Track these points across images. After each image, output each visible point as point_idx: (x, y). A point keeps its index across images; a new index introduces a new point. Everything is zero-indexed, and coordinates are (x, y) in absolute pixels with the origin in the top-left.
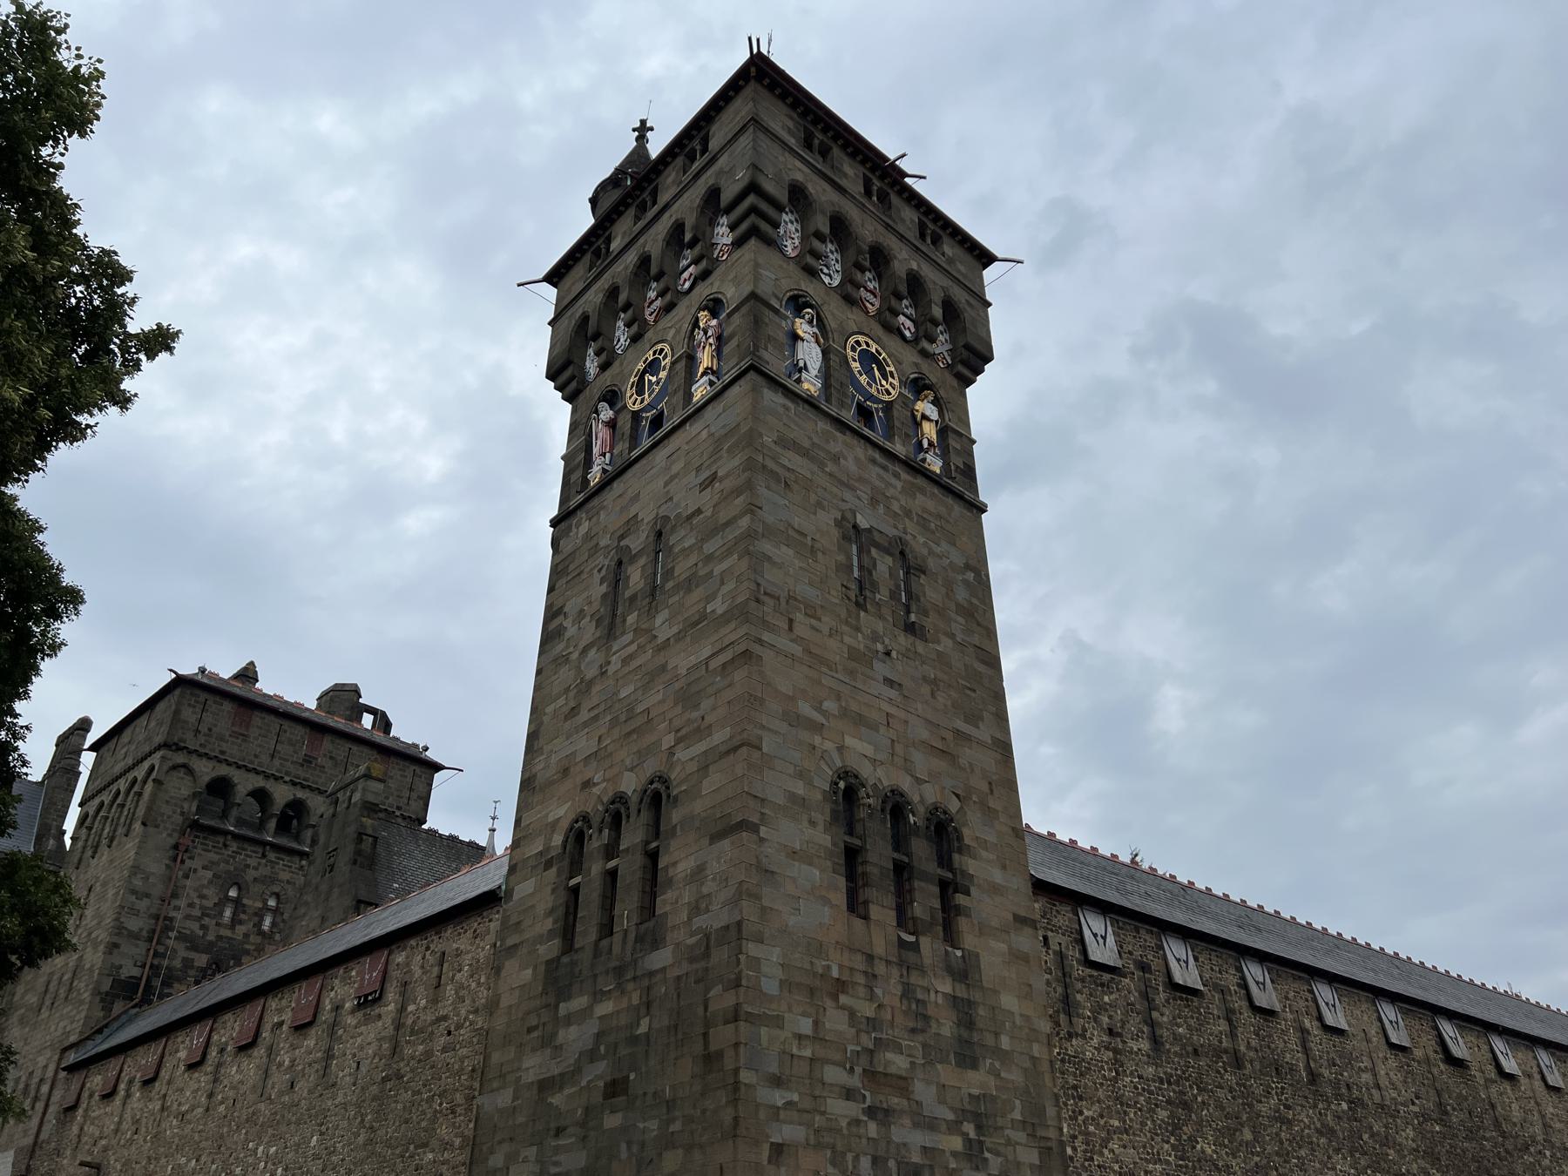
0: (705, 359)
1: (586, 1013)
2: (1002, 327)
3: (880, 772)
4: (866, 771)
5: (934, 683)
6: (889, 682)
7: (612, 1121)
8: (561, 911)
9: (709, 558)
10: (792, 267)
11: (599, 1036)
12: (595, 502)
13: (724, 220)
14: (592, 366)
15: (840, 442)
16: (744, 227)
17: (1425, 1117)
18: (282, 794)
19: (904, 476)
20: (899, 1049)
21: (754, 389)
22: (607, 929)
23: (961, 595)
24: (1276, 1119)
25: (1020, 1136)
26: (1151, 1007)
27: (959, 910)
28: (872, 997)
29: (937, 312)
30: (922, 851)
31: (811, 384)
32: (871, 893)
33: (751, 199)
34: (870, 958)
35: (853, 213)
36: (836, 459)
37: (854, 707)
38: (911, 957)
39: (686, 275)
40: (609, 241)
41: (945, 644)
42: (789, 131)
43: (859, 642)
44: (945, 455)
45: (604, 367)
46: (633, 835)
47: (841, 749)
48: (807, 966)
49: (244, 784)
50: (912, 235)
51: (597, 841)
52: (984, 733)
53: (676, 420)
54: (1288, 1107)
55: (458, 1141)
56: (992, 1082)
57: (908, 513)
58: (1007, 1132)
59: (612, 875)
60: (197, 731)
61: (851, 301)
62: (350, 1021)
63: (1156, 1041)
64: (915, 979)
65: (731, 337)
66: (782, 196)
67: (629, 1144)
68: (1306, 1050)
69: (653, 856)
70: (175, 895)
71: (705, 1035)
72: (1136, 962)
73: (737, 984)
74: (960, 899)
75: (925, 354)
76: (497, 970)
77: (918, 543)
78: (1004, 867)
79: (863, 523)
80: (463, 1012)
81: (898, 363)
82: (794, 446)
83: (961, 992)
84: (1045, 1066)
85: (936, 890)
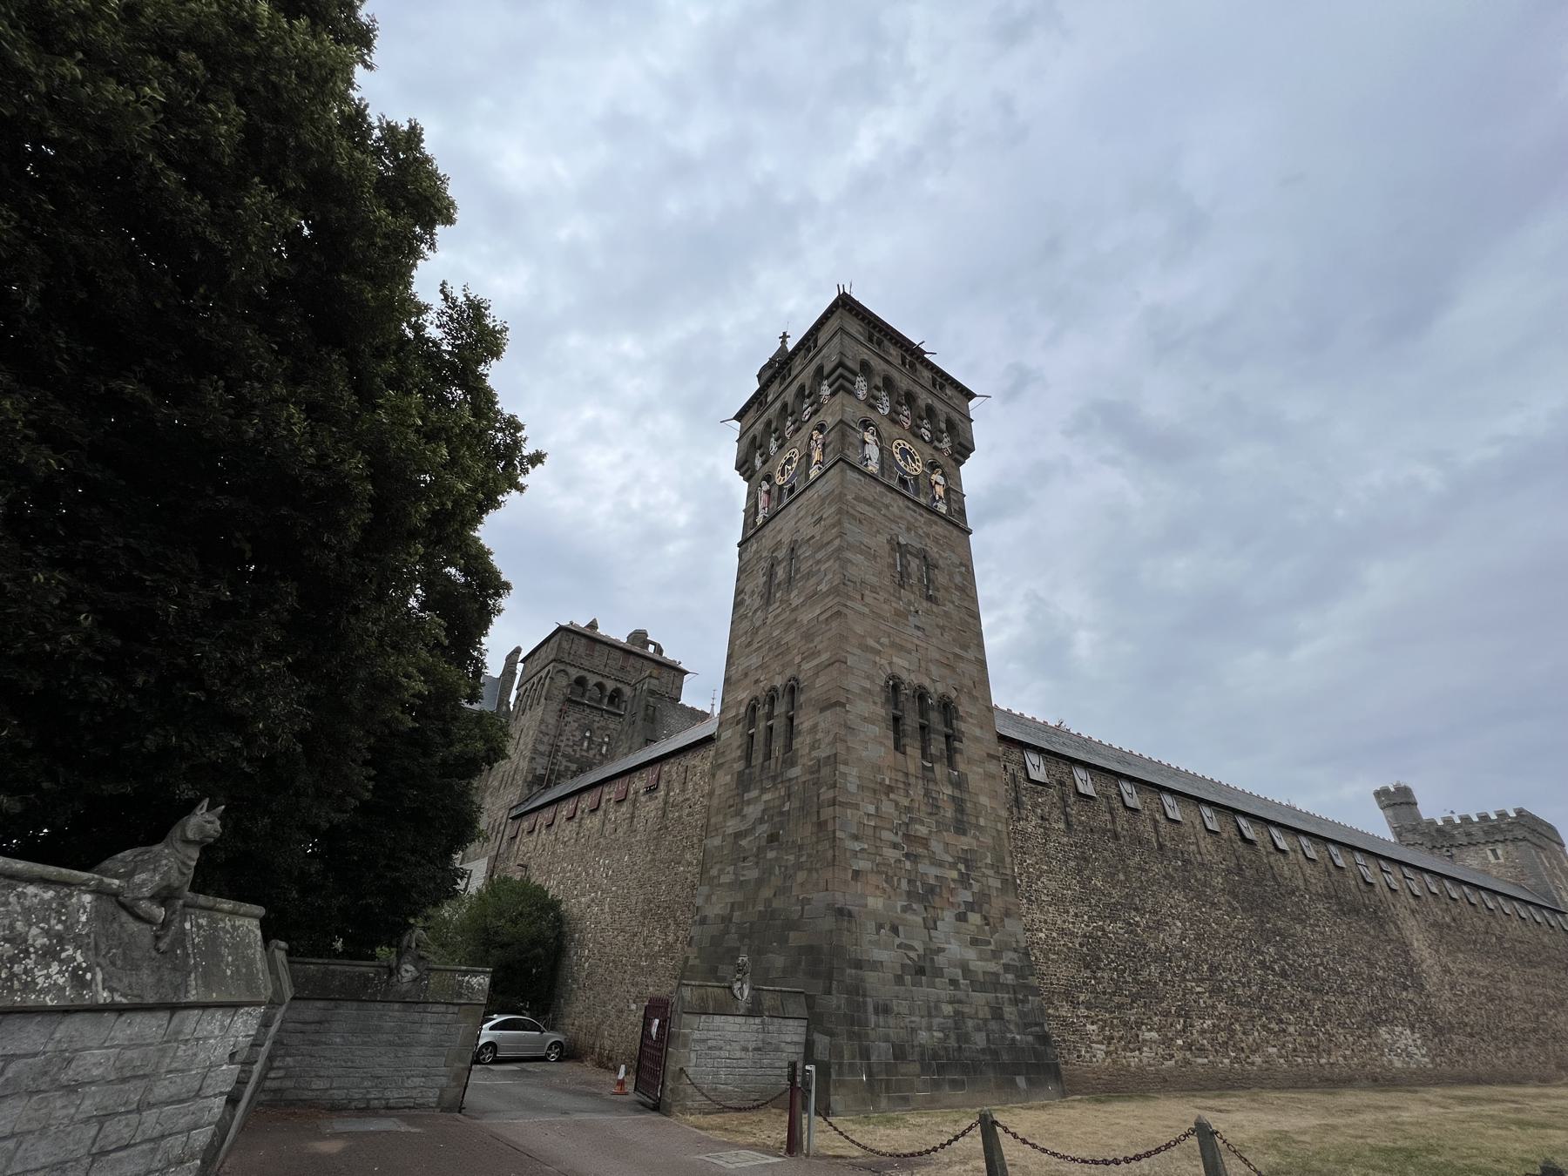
0: (816, 456)
1: (757, 799)
2: (980, 433)
3: (913, 676)
4: (904, 676)
5: (943, 628)
6: (918, 628)
7: (771, 855)
8: (744, 746)
9: (818, 562)
10: (863, 406)
11: (764, 811)
12: (760, 533)
13: (826, 382)
14: (758, 462)
15: (889, 498)
16: (836, 385)
17: (1229, 871)
18: (610, 685)
19: (925, 515)
20: (922, 823)
21: (842, 470)
22: (768, 756)
23: (958, 579)
24: (1139, 869)
25: (990, 872)
26: (1066, 805)
27: (956, 750)
28: (907, 795)
29: (943, 426)
30: (935, 718)
31: (873, 467)
32: (907, 741)
33: (840, 370)
34: (907, 774)
35: (895, 375)
36: (887, 507)
37: (897, 640)
38: (930, 775)
39: (806, 412)
40: (766, 396)
41: (949, 607)
42: (861, 334)
43: (901, 605)
44: (948, 504)
45: (764, 463)
46: (781, 708)
47: (890, 663)
48: (872, 777)
49: (592, 680)
50: (928, 385)
51: (762, 711)
52: (971, 655)
53: (801, 489)
54: (1146, 863)
55: (695, 862)
56: (975, 843)
57: (928, 535)
58: (983, 870)
60: (569, 653)
61: (895, 422)
62: (643, 799)
63: (1068, 824)
64: (931, 786)
65: (830, 443)
66: (857, 368)
67: (780, 867)
68: (1157, 832)
69: (791, 719)
70: (560, 735)
71: (818, 812)
72: (1057, 780)
73: (834, 786)
74: (957, 744)
75: (936, 448)
76: (714, 776)
77: (934, 551)
78: (982, 728)
79: (902, 541)
80: (697, 797)
81: (921, 454)
82: (865, 501)
83: (957, 794)
84: (1004, 835)
85: (943, 739)
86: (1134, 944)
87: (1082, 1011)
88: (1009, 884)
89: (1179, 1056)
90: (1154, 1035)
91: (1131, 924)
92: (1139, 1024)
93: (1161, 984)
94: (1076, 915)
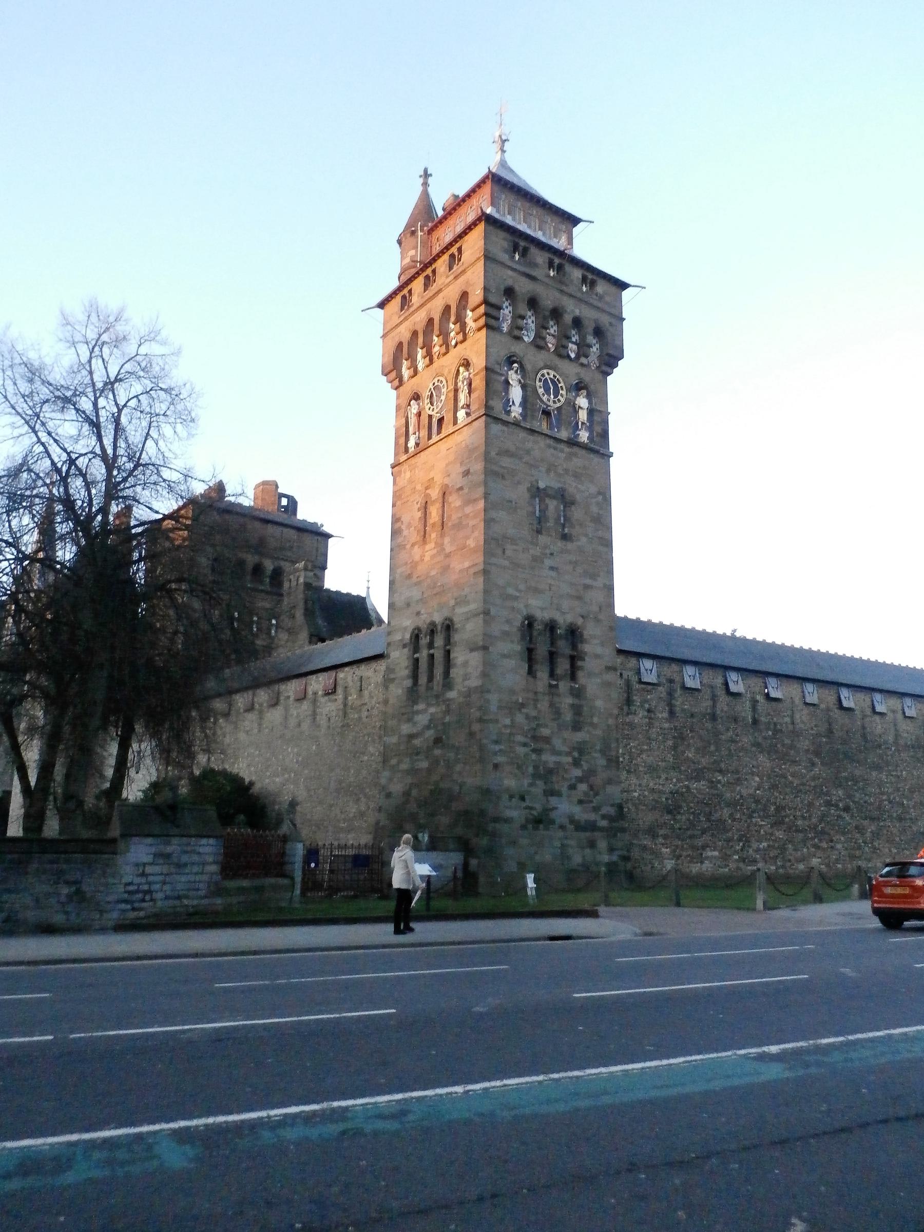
4: (539, 614)
8: (411, 667)
11: (430, 721)
12: (413, 461)
14: (406, 373)
20: (546, 726)
22: (431, 678)
23: (594, 509)
30: (563, 646)
34: (536, 693)
36: (528, 452)
43: (537, 551)
44: (590, 429)
46: (439, 641)
51: (424, 641)
59: (432, 657)
77: (572, 486)
78: (603, 646)
83: (576, 701)
86: (714, 795)
87: (661, 840)
88: (613, 762)
89: (732, 866)
90: (716, 853)
91: (712, 782)
92: (704, 847)
93: (730, 821)
94: (667, 779)
